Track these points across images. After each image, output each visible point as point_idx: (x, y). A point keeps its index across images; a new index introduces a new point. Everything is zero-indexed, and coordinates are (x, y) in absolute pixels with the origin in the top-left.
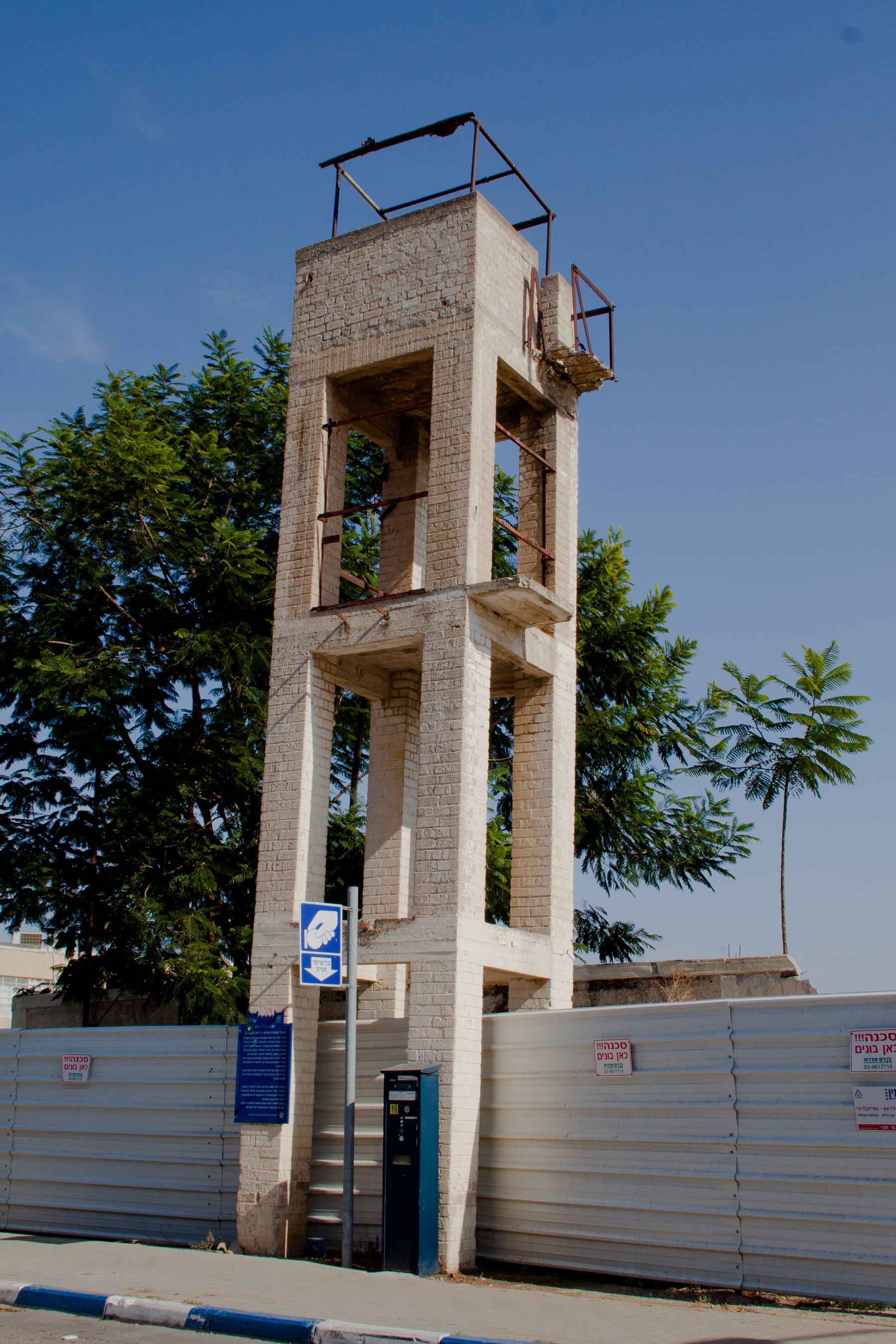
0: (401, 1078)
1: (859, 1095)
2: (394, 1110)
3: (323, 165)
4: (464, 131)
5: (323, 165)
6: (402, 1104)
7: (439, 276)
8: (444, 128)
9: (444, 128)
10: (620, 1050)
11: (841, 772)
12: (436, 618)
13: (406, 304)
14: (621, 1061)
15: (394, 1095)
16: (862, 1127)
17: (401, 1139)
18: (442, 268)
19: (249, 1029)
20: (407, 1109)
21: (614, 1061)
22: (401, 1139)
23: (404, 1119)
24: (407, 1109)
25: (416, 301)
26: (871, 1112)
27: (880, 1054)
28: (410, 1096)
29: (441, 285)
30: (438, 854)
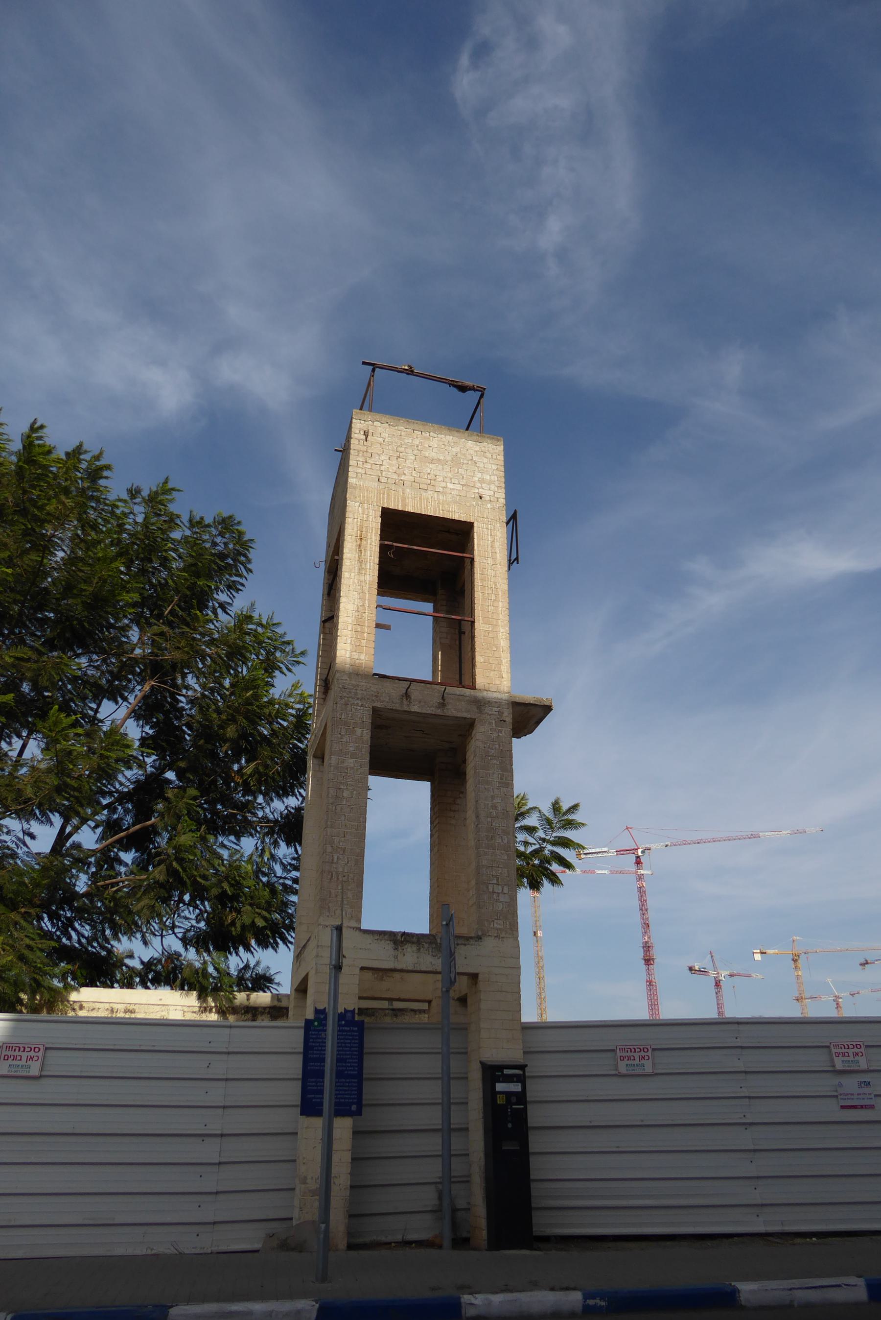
0: (506, 1072)
1: (840, 1085)
2: (501, 1100)
3: (364, 363)
4: (474, 396)
5: (364, 363)
6: (508, 1094)
7: (476, 479)
8: (463, 389)
9: (463, 389)
11: (554, 880)
12: (487, 710)
13: (450, 486)
14: (643, 1062)
15: (500, 1087)
16: (843, 1107)
17: (510, 1125)
18: (479, 475)
19: (316, 1024)
20: (514, 1099)
21: (637, 1062)
22: (510, 1125)
23: (511, 1108)
24: (514, 1099)
25: (459, 487)
26: (850, 1096)
27: (851, 1058)
28: (516, 1087)
30: (498, 889)
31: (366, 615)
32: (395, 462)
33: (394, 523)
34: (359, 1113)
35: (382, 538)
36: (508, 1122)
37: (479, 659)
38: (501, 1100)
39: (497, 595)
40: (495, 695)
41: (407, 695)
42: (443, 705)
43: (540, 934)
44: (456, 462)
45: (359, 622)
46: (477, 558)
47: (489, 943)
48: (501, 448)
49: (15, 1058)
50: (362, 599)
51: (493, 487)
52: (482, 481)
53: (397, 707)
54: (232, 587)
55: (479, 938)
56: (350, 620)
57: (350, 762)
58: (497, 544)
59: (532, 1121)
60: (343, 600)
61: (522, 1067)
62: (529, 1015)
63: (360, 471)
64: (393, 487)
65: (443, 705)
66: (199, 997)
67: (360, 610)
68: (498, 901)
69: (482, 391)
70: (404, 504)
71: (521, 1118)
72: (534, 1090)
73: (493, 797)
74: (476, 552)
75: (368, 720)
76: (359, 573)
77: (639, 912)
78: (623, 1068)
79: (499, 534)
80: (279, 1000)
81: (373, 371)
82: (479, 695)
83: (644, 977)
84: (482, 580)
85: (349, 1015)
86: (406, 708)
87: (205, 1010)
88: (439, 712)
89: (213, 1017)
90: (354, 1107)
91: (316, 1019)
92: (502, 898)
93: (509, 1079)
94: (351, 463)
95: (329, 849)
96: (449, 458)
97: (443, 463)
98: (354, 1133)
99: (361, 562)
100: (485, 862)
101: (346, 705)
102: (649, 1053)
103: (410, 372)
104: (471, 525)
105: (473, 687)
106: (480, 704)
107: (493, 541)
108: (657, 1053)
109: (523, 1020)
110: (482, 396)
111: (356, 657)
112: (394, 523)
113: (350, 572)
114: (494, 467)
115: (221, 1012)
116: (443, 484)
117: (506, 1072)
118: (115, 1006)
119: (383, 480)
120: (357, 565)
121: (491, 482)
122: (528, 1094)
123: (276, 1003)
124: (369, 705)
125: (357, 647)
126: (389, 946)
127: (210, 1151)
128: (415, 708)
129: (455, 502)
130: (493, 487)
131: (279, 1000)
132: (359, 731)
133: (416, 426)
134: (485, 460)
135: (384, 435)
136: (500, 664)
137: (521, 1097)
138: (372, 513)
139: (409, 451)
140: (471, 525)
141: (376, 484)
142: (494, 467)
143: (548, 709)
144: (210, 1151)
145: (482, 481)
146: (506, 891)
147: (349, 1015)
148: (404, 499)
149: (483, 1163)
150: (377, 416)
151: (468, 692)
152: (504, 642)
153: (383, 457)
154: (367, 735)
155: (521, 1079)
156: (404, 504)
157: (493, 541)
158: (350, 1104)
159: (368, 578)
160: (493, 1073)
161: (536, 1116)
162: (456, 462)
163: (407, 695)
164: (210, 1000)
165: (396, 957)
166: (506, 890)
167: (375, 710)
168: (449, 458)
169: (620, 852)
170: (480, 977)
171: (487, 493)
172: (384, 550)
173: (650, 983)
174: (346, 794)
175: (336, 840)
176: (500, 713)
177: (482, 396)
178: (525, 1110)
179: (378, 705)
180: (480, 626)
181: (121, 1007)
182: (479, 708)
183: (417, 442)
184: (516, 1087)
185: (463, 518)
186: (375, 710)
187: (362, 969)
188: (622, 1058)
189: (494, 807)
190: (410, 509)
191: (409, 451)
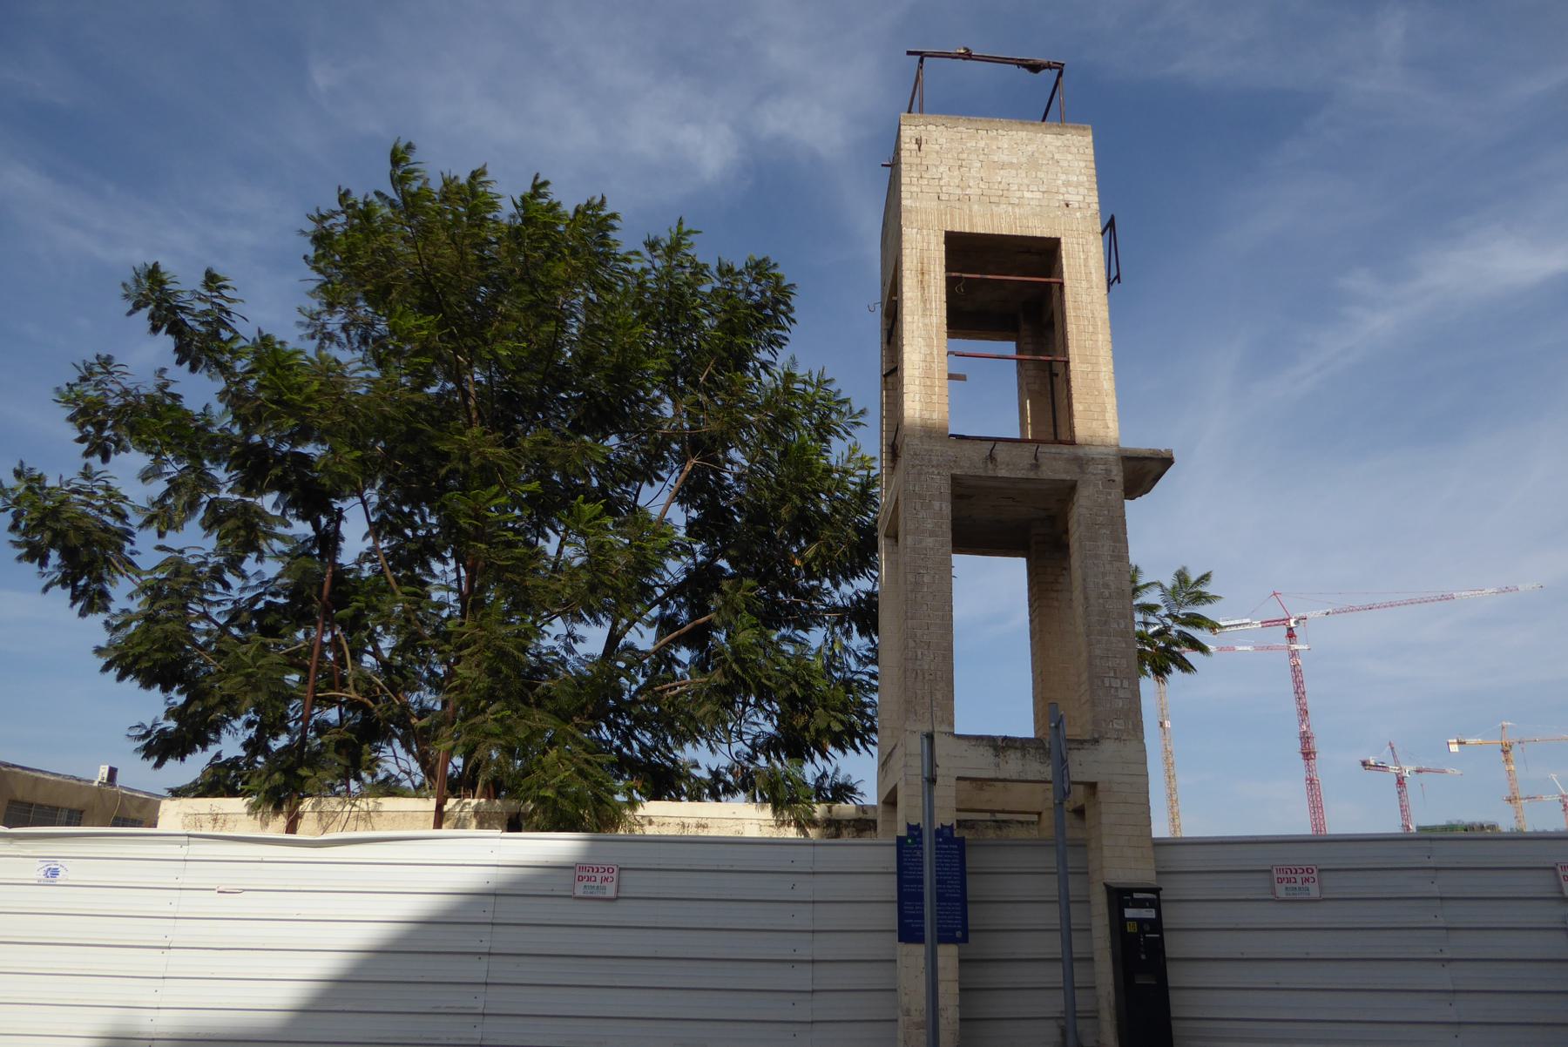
0: (1136, 896)
3: (909, 53)
4: (1049, 76)
5: (909, 53)
6: (1141, 922)
8: (1035, 68)
9: (1035, 68)
10: (1305, 875)
11: (1186, 667)
12: (1091, 469)
13: (1027, 195)
15: (1130, 913)
18: (1064, 177)
20: (1147, 927)
24: (1147, 927)
25: (1038, 195)
28: (1150, 914)
29: (1063, 190)
31: (935, 366)
32: (956, 173)
33: (964, 250)
34: (965, 939)
35: (948, 268)
36: (1142, 955)
37: (1077, 407)
38: (1131, 928)
39: (1095, 326)
40: (1102, 449)
41: (991, 457)
42: (1036, 466)
43: (1167, 724)
44: (1033, 163)
45: (927, 374)
46: (1067, 283)
47: (1108, 748)
48: (1090, 138)
49: (589, 879)
50: (929, 346)
51: (1082, 190)
52: (1067, 184)
53: (981, 472)
54: (775, 343)
55: (1096, 741)
56: (917, 373)
57: (929, 542)
58: (1092, 263)
59: (1170, 951)
60: (906, 349)
61: (1156, 891)
62: (1160, 829)
63: (914, 189)
64: (957, 205)
65: (1036, 466)
66: (775, 811)
67: (928, 361)
68: (1116, 697)
69: (1060, 67)
70: (971, 225)
71: (1157, 948)
72: (1171, 916)
73: (1104, 574)
74: (1066, 275)
75: (946, 490)
76: (924, 315)
77: (1293, 697)
78: (1281, 893)
79: (1093, 249)
80: (864, 812)
81: (921, 61)
82: (1081, 452)
83: (1303, 774)
84: (1075, 309)
85: (947, 831)
86: (991, 473)
87: (782, 824)
88: (1032, 475)
89: (791, 833)
90: (959, 934)
91: (909, 836)
92: (1121, 694)
93: (1140, 904)
94: (904, 180)
95: (912, 644)
96: (1023, 160)
97: (1018, 167)
98: (961, 961)
99: (924, 301)
100: (1098, 652)
101: (920, 474)
102: (1315, 875)
103: (968, 56)
104: (1056, 243)
105: (1072, 443)
106: (1081, 462)
107: (1086, 260)
108: (1325, 875)
109: (1155, 835)
110: (1060, 74)
111: (927, 416)
112: (964, 250)
113: (913, 314)
114: (1082, 164)
115: (799, 825)
116: (1018, 194)
117: (1136, 896)
118: (686, 821)
119: (943, 197)
120: (921, 306)
121: (1079, 184)
122: (1164, 920)
123: (861, 815)
124: (946, 473)
125: (928, 404)
126: (988, 753)
127: (801, 978)
128: (1002, 473)
129: (1035, 215)
130: (1082, 190)
131: (864, 812)
132: (936, 505)
133: (980, 125)
134: (1070, 157)
135: (942, 141)
136: (1104, 411)
137: (1156, 925)
138: (933, 240)
139: (973, 156)
140: (1056, 243)
141: (935, 203)
142: (1082, 164)
143: (1166, 462)
144: (801, 978)
145: (1067, 184)
146: (1126, 684)
147: (947, 831)
148: (971, 220)
149: (1112, 998)
150: (930, 118)
151: (1066, 449)
152: (1107, 383)
153: (941, 169)
154: (947, 508)
155: (1156, 904)
156: (971, 225)
157: (1086, 260)
158: (955, 930)
159: (934, 320)
160: (1120, 897)
161: (1174, 946)
162: (1033, 163)
163: (991, 457)
164: (786, 813)
165: (998, 765)
166: (1126, 684)
167: (954, 478)
168: (1023, 160)
169: (1266, 623)
170: (1100, 786)
171: (1074, 199)
172: (951, 283)
173: (1311, 781)
174: (926, 579)
175: (919, 633)
176: (1108, 471)
177: (1060, 74)
178: (1161, 939)
179: (958, 472)
180: (1076, 367)
181: (693, 822)
182: (1081, 467)
183: (982, 144)
184: (1150, 914)
185: (1047, 233)
186: (954, 478)
187: (959, 779)
188: (1281, 881)
189: (1106, 586)
190: (980, 230)
191: (973, 156)
